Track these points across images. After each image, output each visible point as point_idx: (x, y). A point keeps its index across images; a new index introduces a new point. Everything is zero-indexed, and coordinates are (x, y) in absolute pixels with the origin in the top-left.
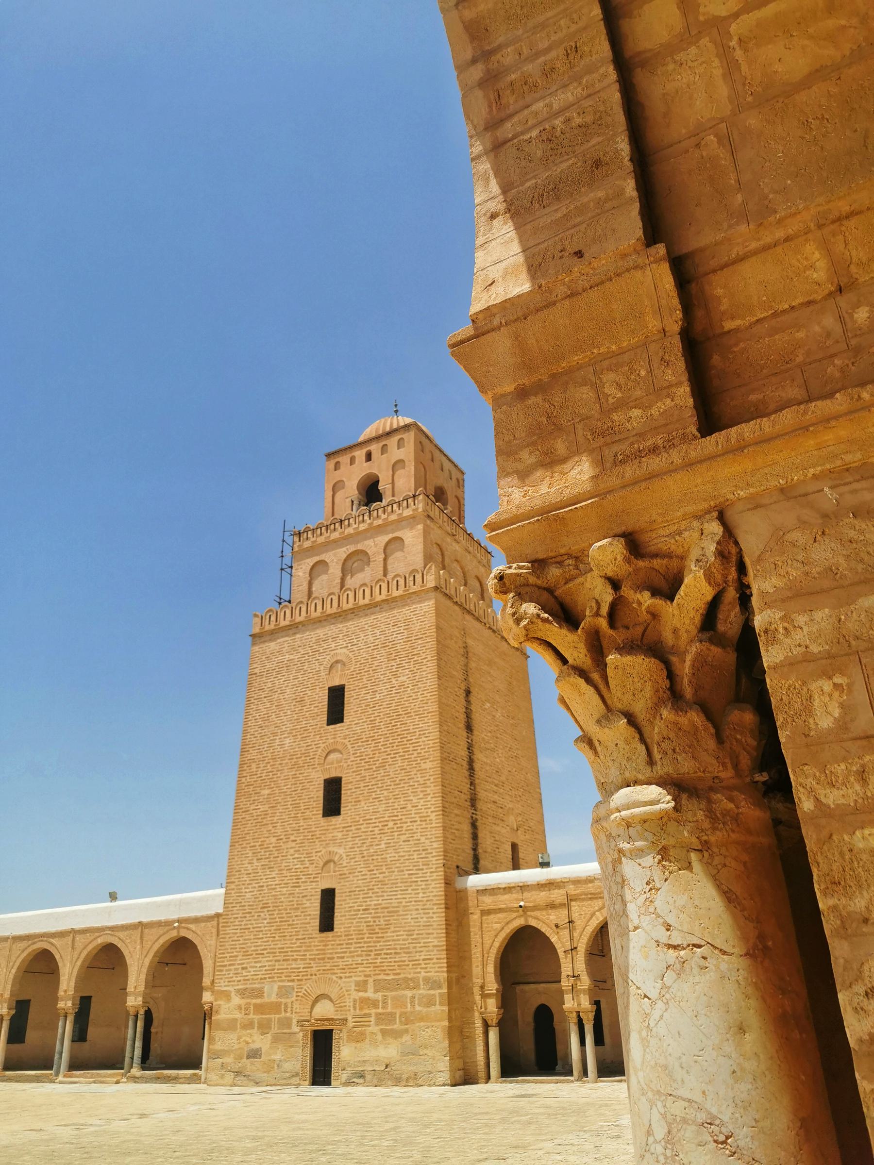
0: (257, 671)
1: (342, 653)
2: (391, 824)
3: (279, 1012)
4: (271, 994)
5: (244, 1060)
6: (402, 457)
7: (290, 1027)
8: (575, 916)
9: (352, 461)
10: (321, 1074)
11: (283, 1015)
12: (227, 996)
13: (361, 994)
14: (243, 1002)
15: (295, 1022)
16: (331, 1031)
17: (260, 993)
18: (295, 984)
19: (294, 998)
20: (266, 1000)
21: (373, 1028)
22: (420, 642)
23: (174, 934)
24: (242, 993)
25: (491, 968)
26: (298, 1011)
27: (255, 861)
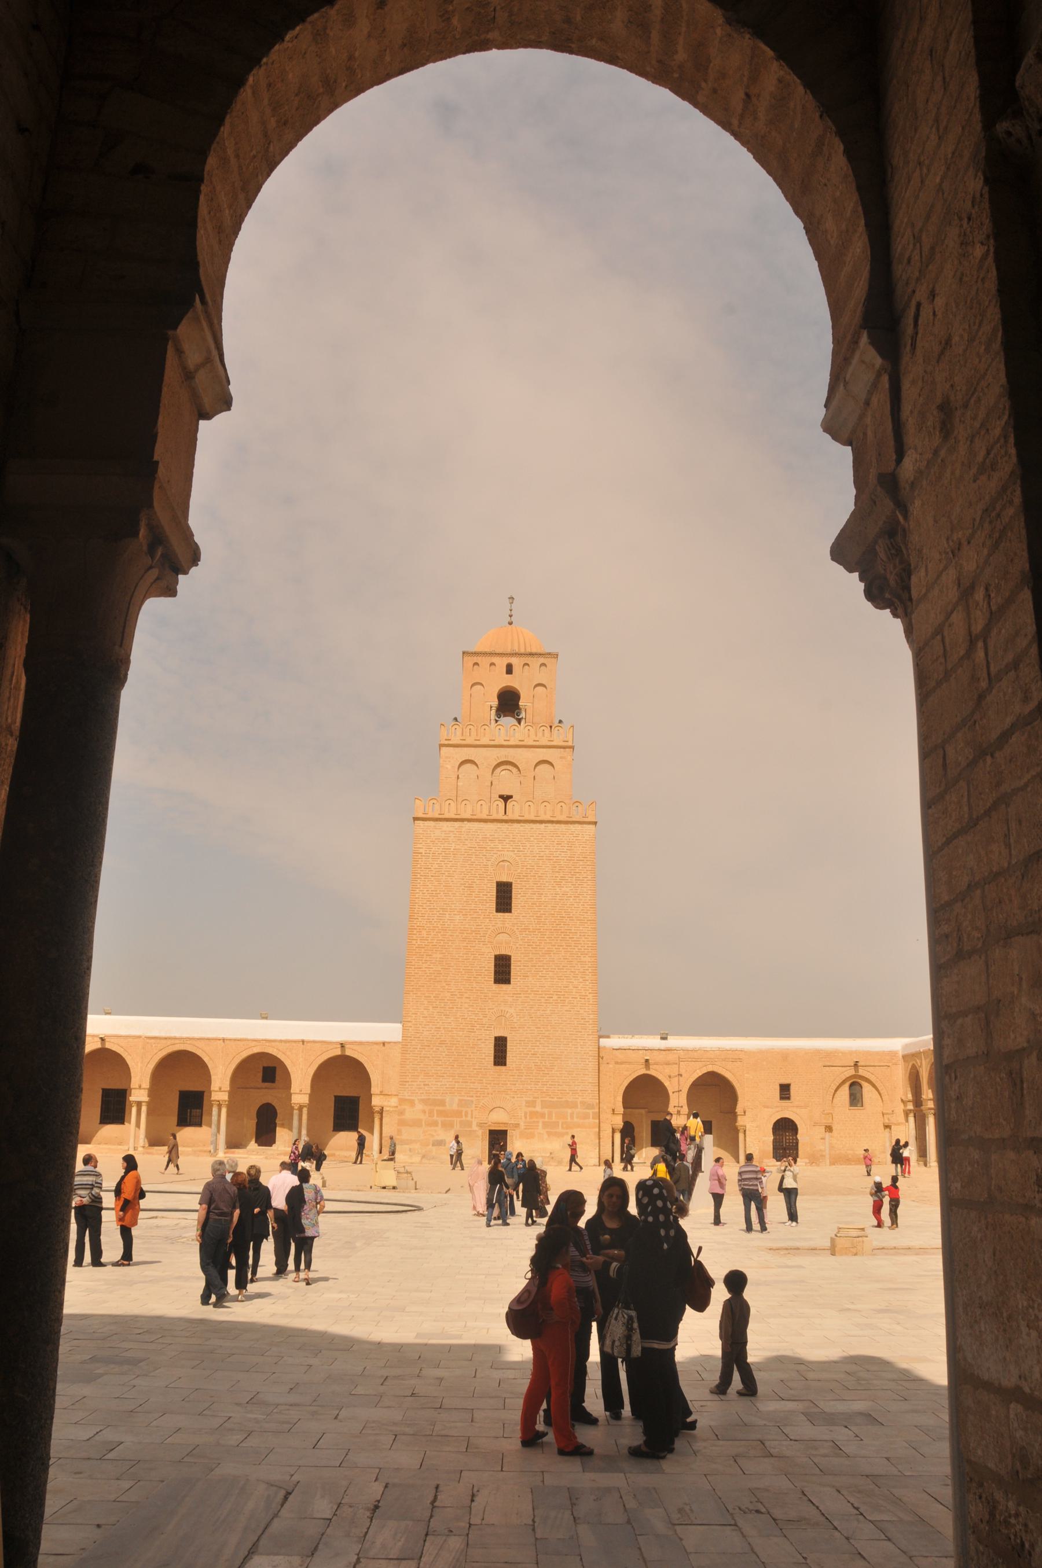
0: (421, 851)
2: (555, 997)
8: (682, 1072)
12: (412, 1103)
16: (505, 1132)
17: (442, 1103)
18: (474, 1099)
22: (581, 863)
24: (425, 1101)
25: (620, 1099)
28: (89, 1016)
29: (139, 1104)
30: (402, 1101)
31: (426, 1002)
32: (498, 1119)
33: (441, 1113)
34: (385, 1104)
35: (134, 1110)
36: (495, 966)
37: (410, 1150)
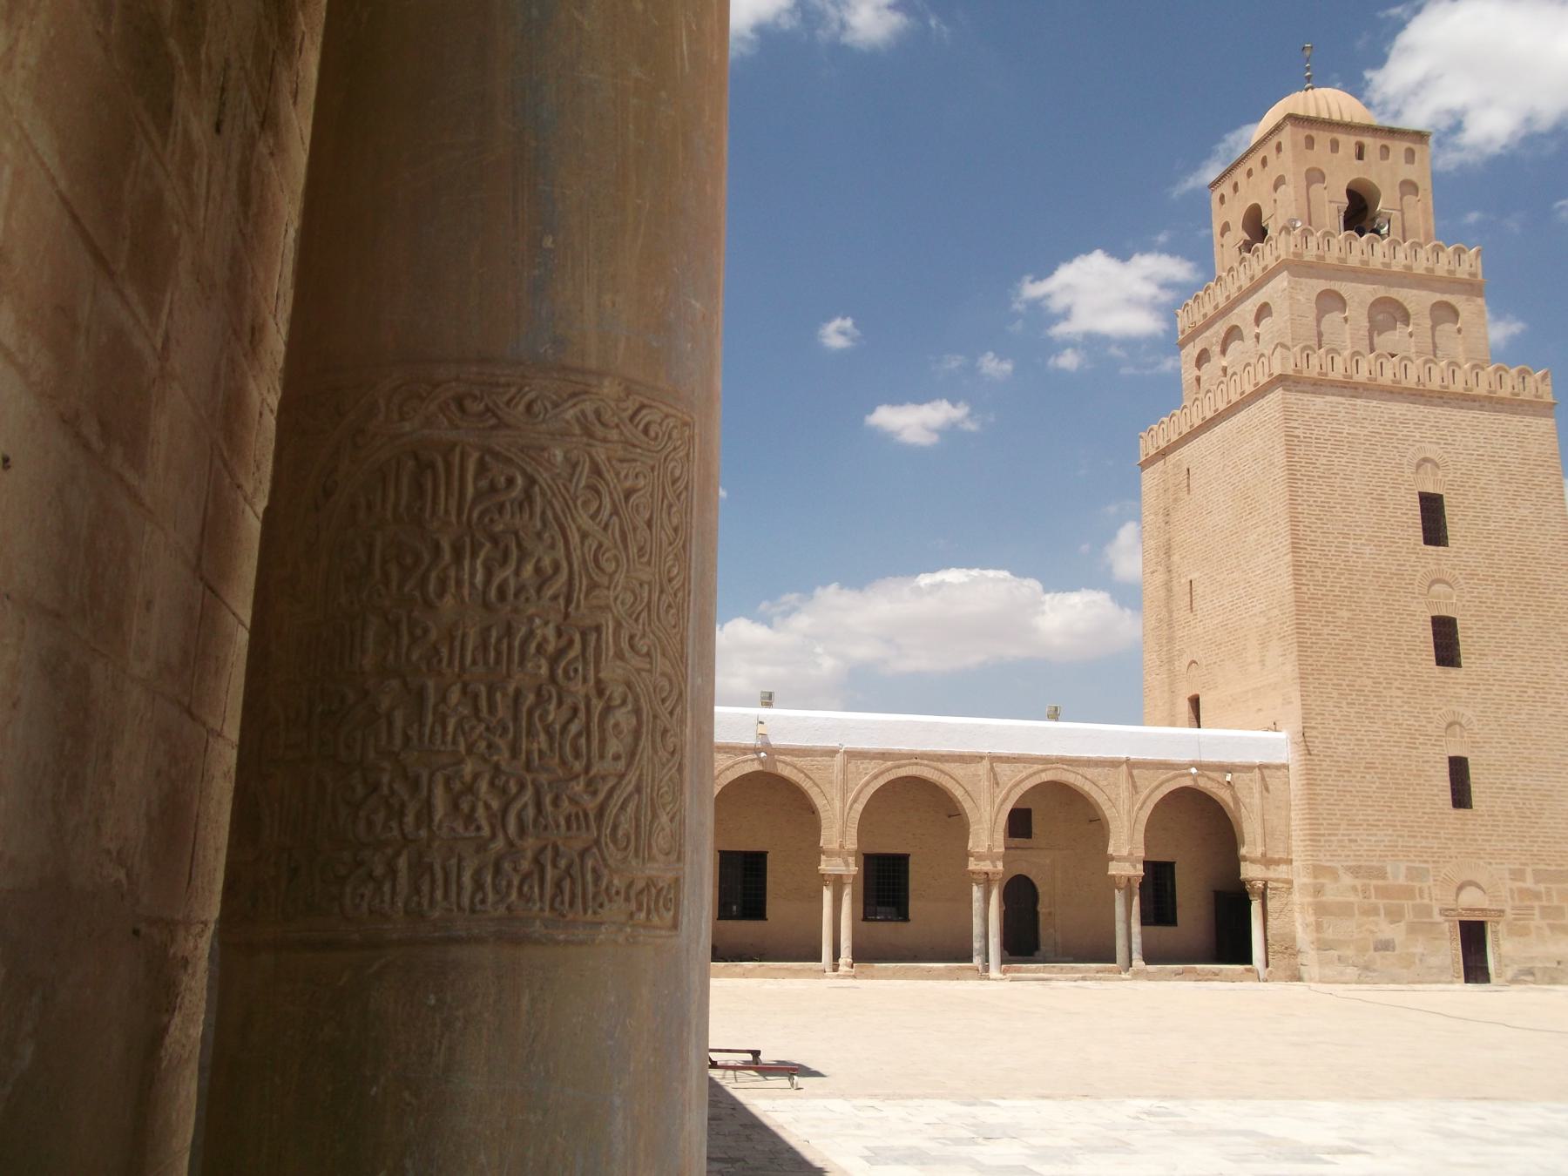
0: (1297, 432)
1: (1433, 451)
2: (1531, 692)
3: (1412, 897)
4: (1397, 874)
5: (1371, 952)
6: (1414, 178)
7: (1430, 915)
9: (1335, 146)
10: (1475, 969)
11: (1418, 901)
12: (1333, 873)
13: (1520, 884)
14: (1358, 883)
15: (1436, 911)
17: (1381, 874)
18: (1430, 866)
19: (1431, 882)
20: (1390, 881)
21: (1537, 921)
22: (1541, 470)
23: (1187, 782)
24: (1355, 871)
26: (1437, 897)
27: (1344, 704)
28: (717, 709)
29: (838, 882)
30: (1317, 870)
31: (1335, 694)
32: (1472, 901)
33: (1383, 892)
34: (1271, 874)
35: (827, 895)
36: (1435, 634)
37: (1339, 958)
